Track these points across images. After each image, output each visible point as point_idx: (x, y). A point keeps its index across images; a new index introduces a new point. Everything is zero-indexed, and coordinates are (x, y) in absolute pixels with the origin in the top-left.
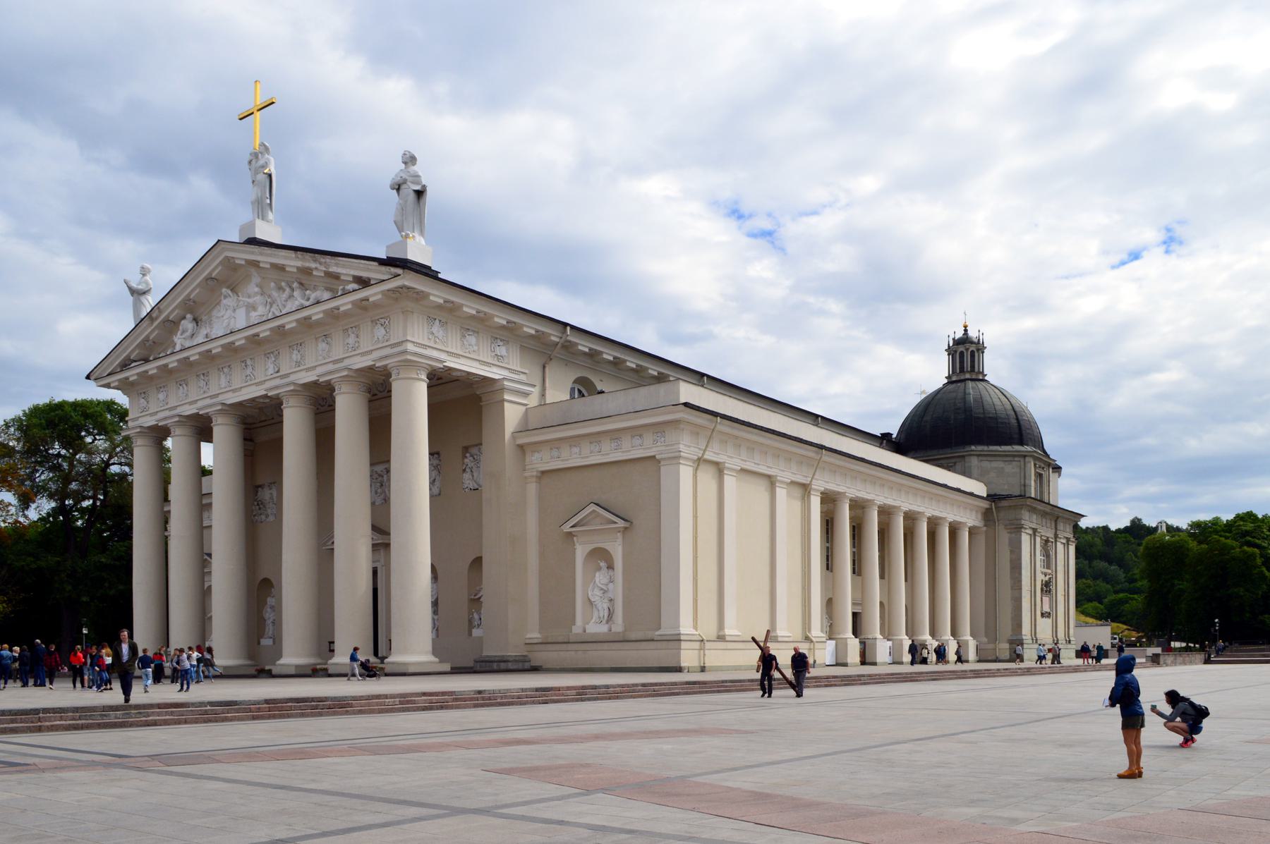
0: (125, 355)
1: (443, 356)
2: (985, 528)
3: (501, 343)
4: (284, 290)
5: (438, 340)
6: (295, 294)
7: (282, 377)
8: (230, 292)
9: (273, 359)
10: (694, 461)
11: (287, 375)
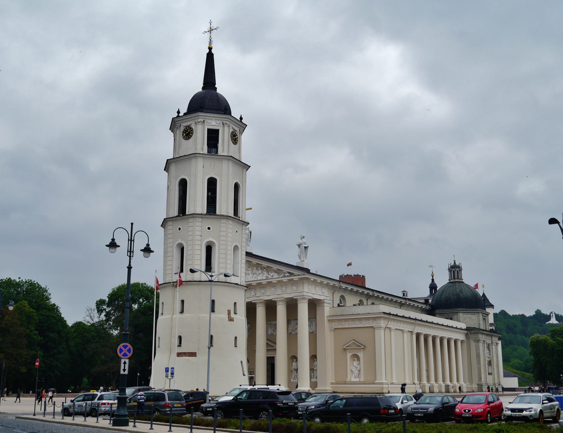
2: (466, 341)
4: (258, 270)
7: (257, 297)
9: (254, 291)
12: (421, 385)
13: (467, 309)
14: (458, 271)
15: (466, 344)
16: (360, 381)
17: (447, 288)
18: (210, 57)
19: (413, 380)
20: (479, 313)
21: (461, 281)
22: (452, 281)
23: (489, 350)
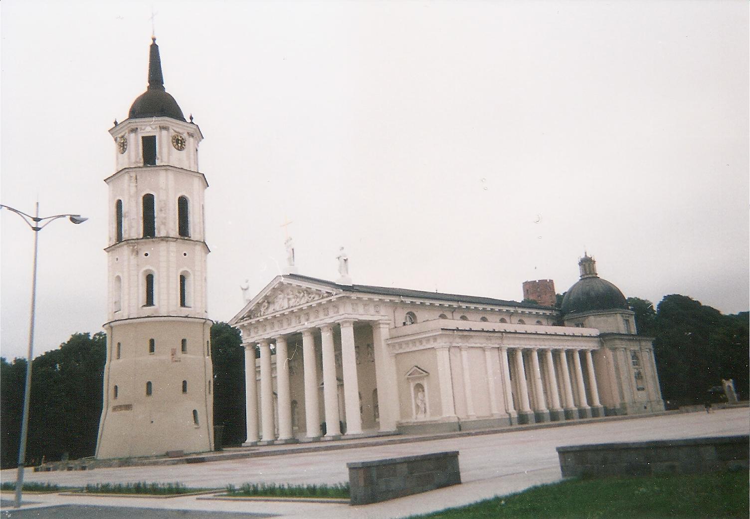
6: (305, 295)
18: (154, 50)
21: (594, 275)
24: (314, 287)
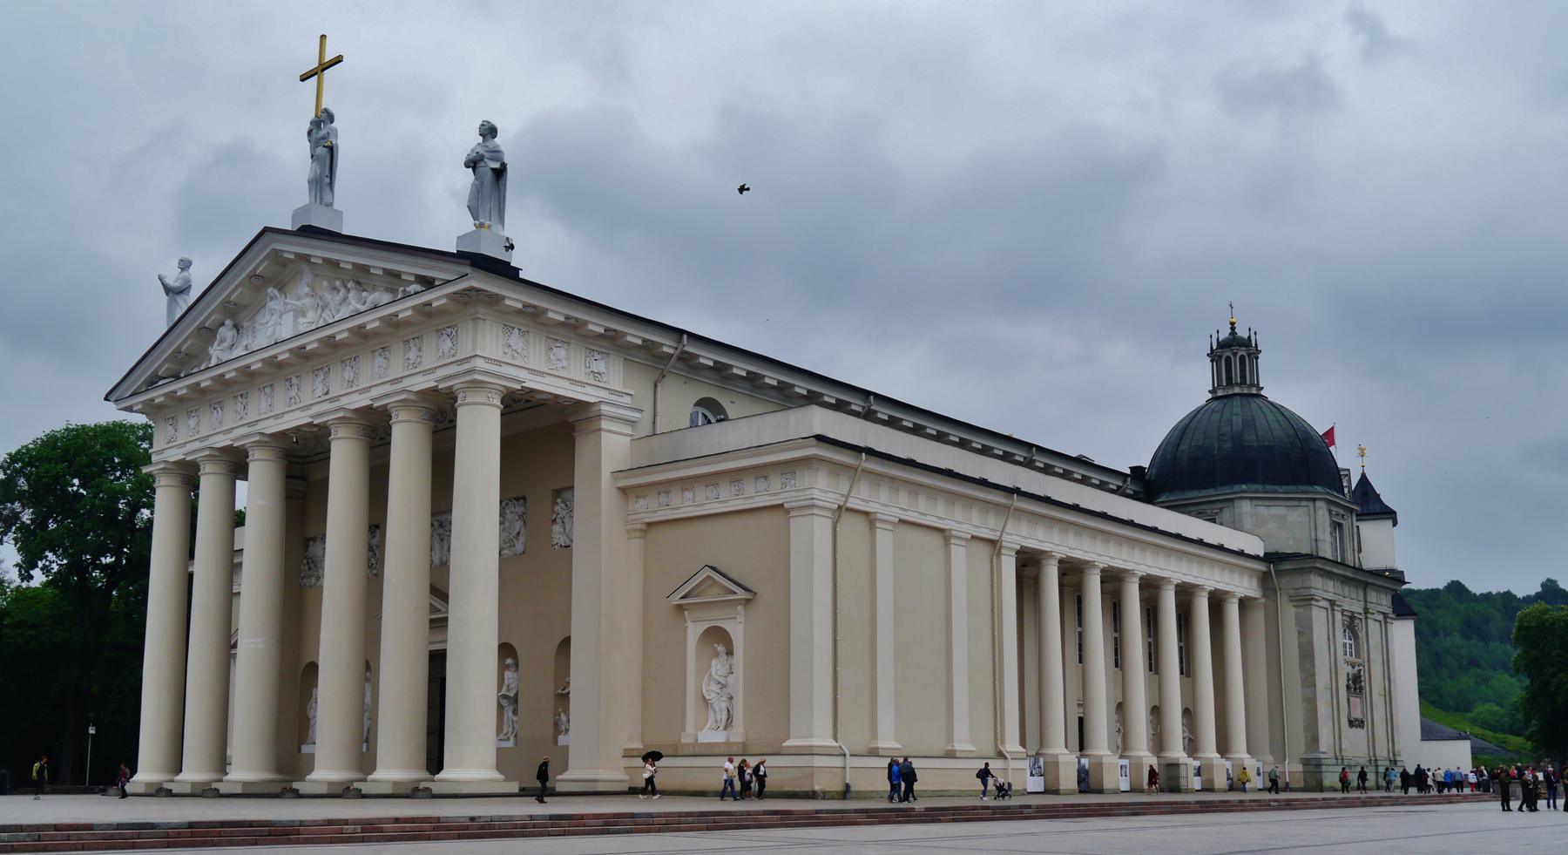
0: (151, 371)
1: (522, 375)
2: (1263, 600)
3: (599, 357)
4: (339, 291)
5: (516, 355)
6: (351, 295)
7: (332, 400)
8: (276, 292)
9: (322, 377)
10: (833, 511)
11: (337, 398)
12: (1042, 760)
13: (1268, 487)
14: (1242, 357)
15: (1262, 612)
16: (731, 740)
17: (1199, 416)
19: (996, 740)
20: (1314, 500)
21: (1254, 391)
22: (1220, 393)
23: (1354, 635)
24: (378, 263)
